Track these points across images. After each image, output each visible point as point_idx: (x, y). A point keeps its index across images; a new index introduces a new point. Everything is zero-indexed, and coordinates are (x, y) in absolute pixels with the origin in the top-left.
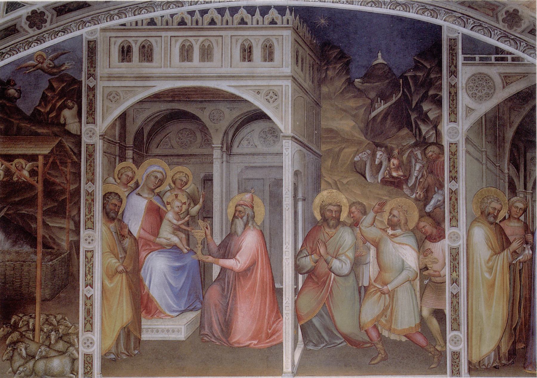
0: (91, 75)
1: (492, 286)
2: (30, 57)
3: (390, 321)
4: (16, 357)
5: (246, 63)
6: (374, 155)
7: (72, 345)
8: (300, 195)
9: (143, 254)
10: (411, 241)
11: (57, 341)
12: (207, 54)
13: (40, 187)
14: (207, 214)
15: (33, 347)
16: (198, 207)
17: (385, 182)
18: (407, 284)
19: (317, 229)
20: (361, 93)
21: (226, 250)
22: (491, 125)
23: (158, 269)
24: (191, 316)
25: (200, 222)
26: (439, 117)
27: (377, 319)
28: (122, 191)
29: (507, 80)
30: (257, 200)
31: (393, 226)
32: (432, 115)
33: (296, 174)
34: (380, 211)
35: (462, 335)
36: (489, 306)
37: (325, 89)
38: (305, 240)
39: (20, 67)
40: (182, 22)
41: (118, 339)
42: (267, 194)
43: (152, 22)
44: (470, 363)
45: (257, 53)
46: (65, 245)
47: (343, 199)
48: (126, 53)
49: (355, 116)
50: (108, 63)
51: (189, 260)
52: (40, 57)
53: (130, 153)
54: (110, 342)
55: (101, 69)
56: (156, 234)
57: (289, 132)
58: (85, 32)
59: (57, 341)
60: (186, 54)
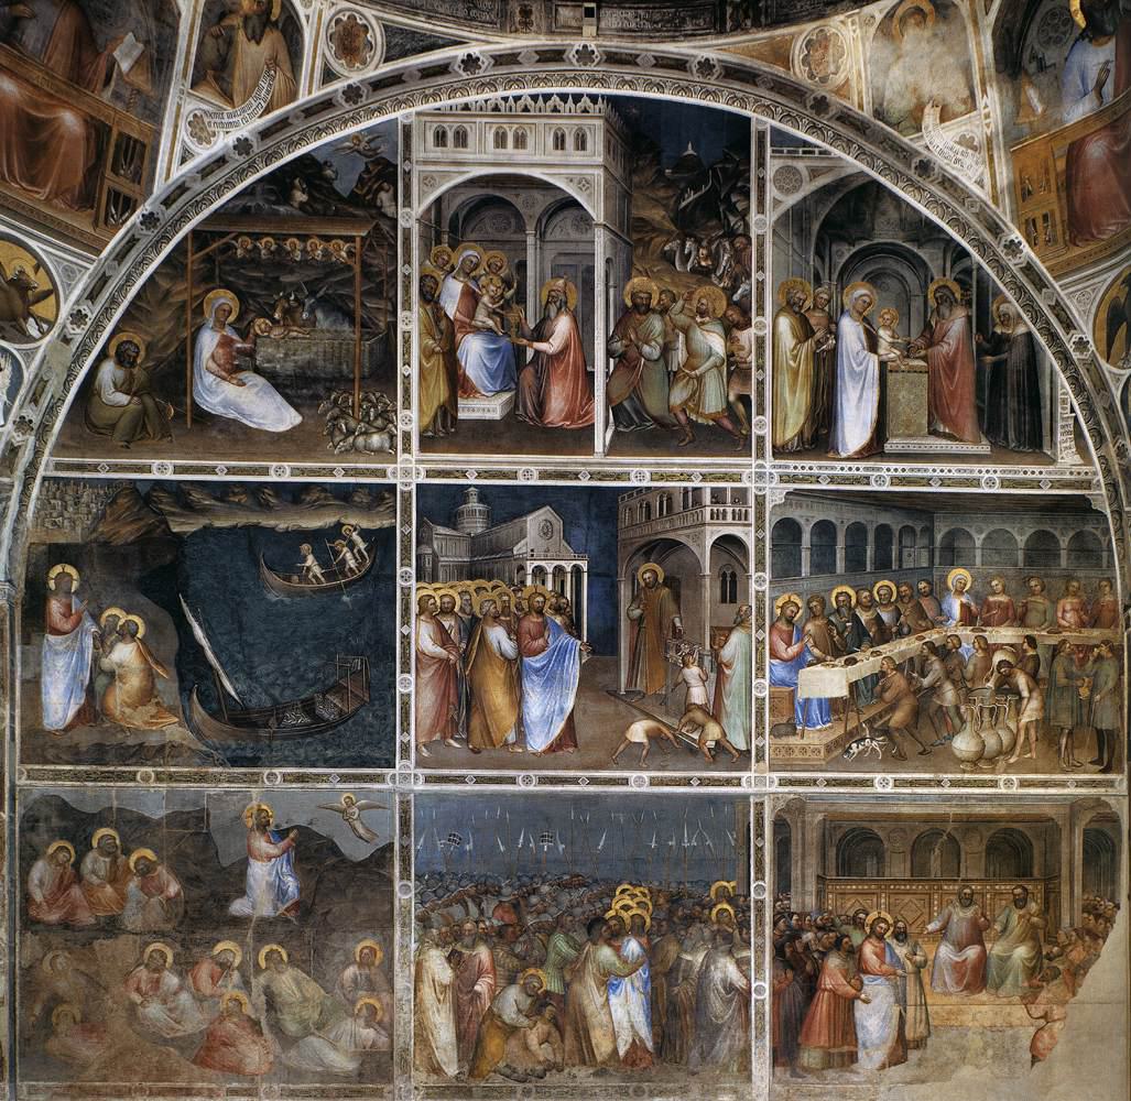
0: (407, 158)
1: (796, 373)
2: (346, 138)
3: (698, 405)
4: (337, 433)
5: (559, 152)
6: (683, 245)
7: (392, 422)
8: (611, 283)
9: (459, 336)
10: (719, 329)
11: (376, 418)
12: (520, 141)
13: (357, 268)
14: (521, 297)
15: (352, 423)
16: (512, 291)
17: (693, 270)
18: (715, 371)
19: (630, 314)
20: (670, 184)
21: (541, 334)
22: (796, 220)
23: (473, 351)
24: (506, 396)
25: (514, 306)
26: (747, 210)
27: (686, 402)
28: (439, 275)
29: (814, 173)
30: (571, 285)
31: (702, 314)
32: (740, 206)
33: (608, 261)
34: (689, 299)
35: (767, 418)
36: (793, 392)
37: (636, 179)
38: (616, 326)
39: (334, 146)
40: (496, 108)
41: (435, 419)
42: (580, 280)
43: (466, 107)
44: (774, 447)
45: (570, 141)
46: (382, 324)
47: (654, 286)
48: (440, 138)
49: (665, 207)
50: (423, 148)
51: (504, 342)
52: (356, 137)
53: (445, 237)
54: (427, 420)
55: (417, 153)
56: (472, 316)
57: (602, 221)
58: (400, 115)
59: (376, 418)
60: (500, 140)
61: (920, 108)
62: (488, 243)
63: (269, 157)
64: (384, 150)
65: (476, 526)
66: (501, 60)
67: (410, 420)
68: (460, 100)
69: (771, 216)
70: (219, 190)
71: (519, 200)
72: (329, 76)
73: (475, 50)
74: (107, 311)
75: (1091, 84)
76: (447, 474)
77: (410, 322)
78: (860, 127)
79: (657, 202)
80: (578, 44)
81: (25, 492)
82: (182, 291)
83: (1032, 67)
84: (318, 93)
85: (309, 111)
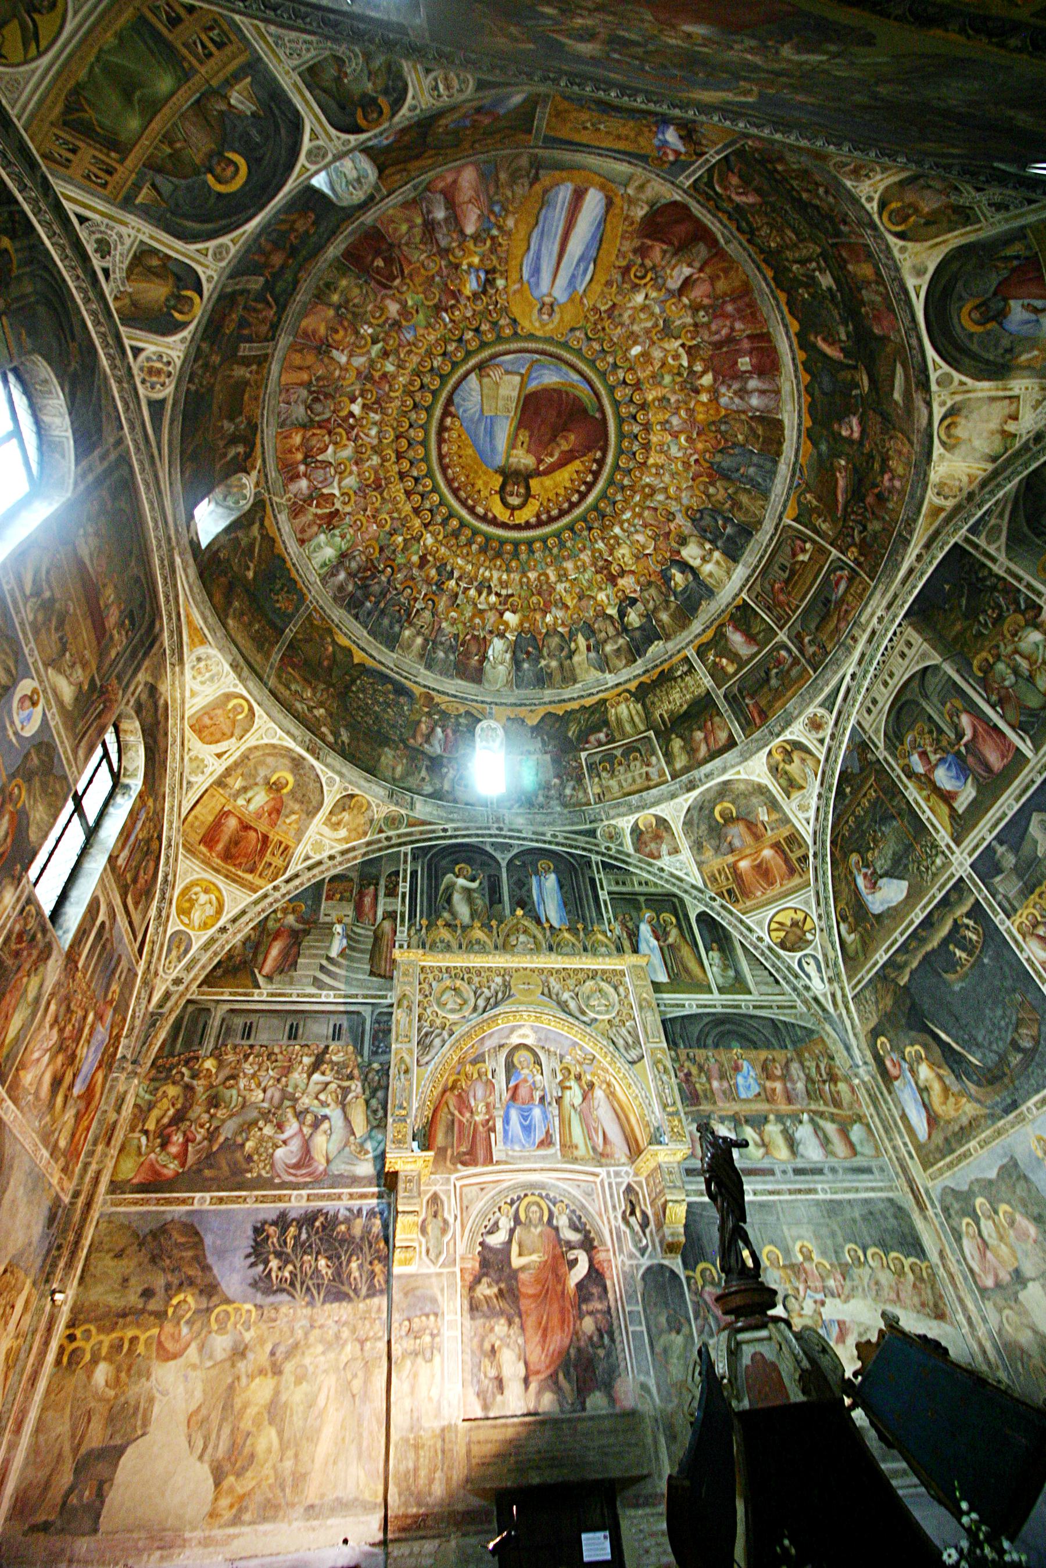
14: (940, 731)
20: (951, 609)
47: (984, 654)
51: (950, 758)
55: (866, 726)
61: (1003, 432)
62: (910, 728)
63: (830, 790)
64: (858, 740)
65: (1010, 860)
66: (859, 663)
67: (943, 837)
68: (863, 691)
69: (1002, 557)
70: (826, 819)
71: (907, 696)
72: (821, 741)
73: (850, 671)
74: (827, 904)
75: (1033, 317)
76: (977, 846)
77: (913, 793)
78: (995, 474)
79: (953, 624)
80: (875, 620)
81: (847, 1009)
82: (841, 869)
83: (1008, 356)
84: (824, 750)
85: (827, 760)
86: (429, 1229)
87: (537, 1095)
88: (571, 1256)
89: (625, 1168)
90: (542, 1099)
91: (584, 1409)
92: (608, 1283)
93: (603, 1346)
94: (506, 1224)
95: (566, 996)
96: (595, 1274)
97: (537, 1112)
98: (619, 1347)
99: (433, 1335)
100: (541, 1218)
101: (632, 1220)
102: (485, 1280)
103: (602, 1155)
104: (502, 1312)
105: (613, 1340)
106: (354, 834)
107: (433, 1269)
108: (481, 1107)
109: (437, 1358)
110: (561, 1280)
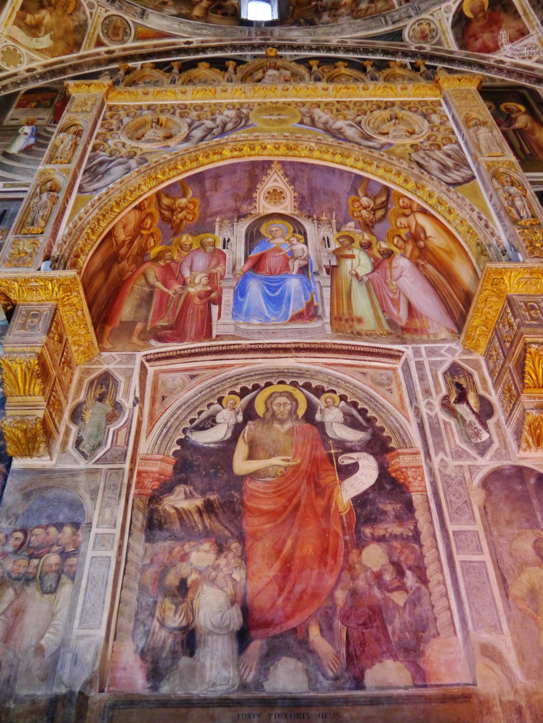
86: (87, 415)
87: (295, 265)
88: (346, 460)
89: (447, 345)
90: (304, 270)
91: (359, 684)
92: (416, 498)
93: (402, 588)
94: (227, 418)
95: (340, 124)
96: (390, 484)
97: (294, 284)
98: (436, 590)
99: (64, 555)
100: (293, 413)
101: (462, 408)
102: (180, 489)
103: (405, 329)
104: (207, 534)
105: (423, 580)
106: (61, 45)
107: (83, 464)
108: (201, 278)
109: (66, 589)
110: (323, 492)
